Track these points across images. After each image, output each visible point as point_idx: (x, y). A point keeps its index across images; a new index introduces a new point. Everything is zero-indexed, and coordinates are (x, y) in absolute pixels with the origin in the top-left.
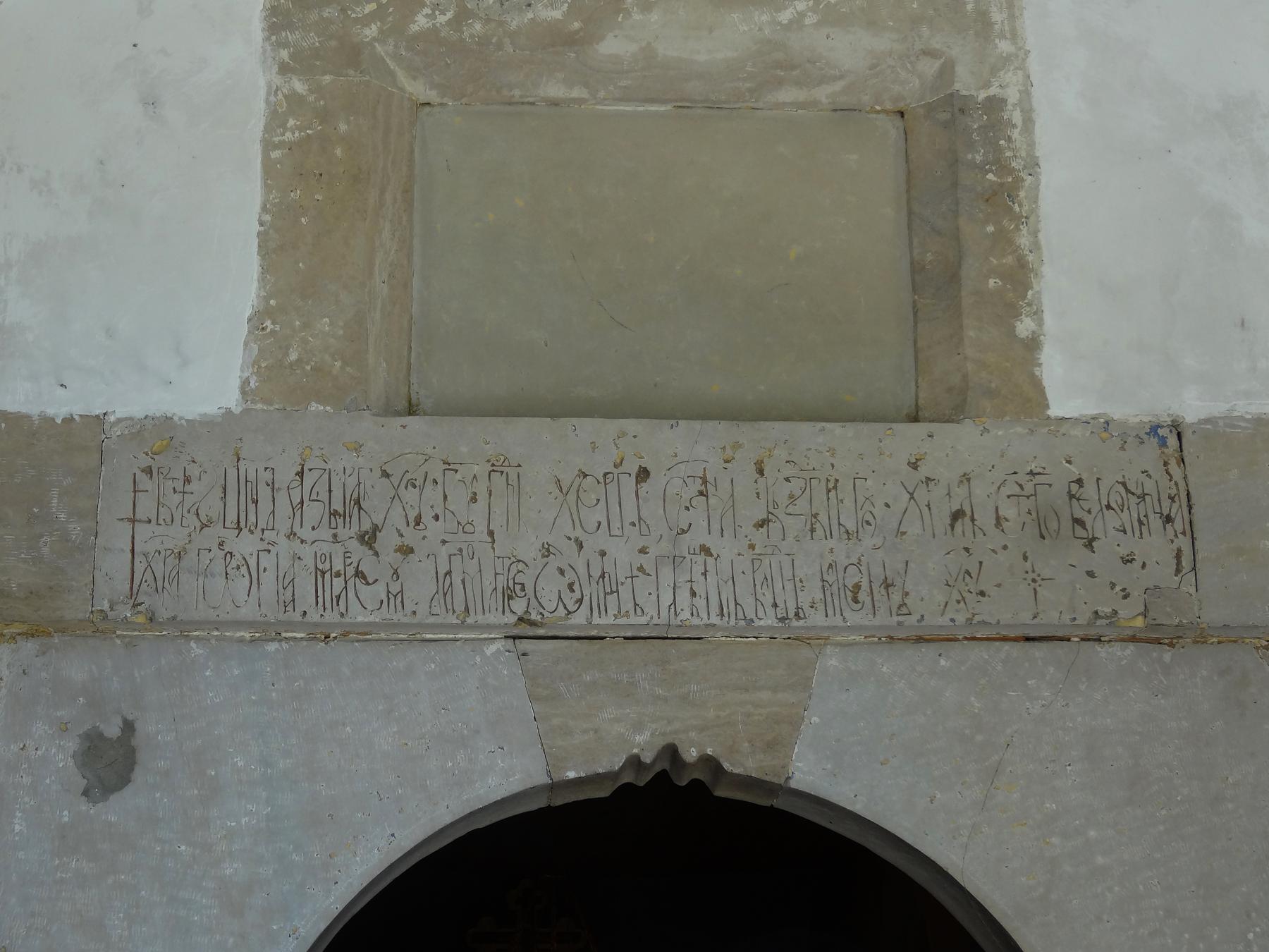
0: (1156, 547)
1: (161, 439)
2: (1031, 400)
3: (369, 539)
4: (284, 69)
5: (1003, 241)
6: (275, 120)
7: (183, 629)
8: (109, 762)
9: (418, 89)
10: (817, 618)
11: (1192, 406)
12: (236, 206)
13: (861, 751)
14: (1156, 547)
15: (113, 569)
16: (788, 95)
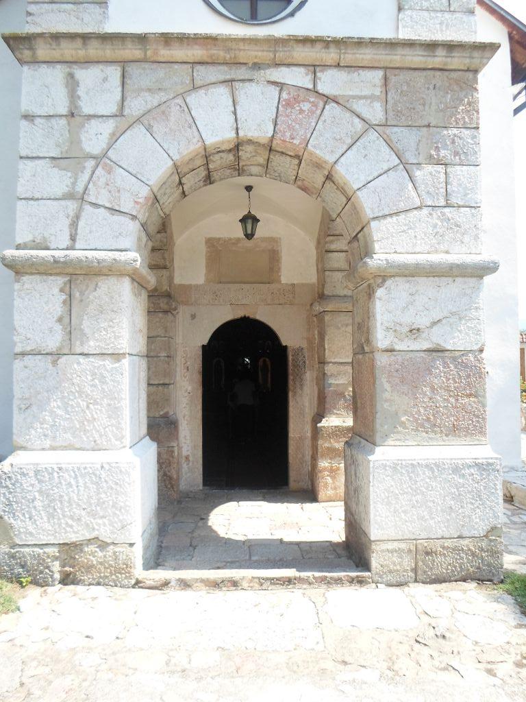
0: (291, 296)
1: (197, 286)
3: (217, 296)
4: (207, 248)
5: (278, 265)
6: (207, 253)
7: (199, 305)
8: (193, 317)
9: (220, 249)
10: (259, 303)
11: (295, 282)
12: (203, 262)
13: (263, 315)
14: (291, 296)
15: (193, 299)
16: (258, 249)
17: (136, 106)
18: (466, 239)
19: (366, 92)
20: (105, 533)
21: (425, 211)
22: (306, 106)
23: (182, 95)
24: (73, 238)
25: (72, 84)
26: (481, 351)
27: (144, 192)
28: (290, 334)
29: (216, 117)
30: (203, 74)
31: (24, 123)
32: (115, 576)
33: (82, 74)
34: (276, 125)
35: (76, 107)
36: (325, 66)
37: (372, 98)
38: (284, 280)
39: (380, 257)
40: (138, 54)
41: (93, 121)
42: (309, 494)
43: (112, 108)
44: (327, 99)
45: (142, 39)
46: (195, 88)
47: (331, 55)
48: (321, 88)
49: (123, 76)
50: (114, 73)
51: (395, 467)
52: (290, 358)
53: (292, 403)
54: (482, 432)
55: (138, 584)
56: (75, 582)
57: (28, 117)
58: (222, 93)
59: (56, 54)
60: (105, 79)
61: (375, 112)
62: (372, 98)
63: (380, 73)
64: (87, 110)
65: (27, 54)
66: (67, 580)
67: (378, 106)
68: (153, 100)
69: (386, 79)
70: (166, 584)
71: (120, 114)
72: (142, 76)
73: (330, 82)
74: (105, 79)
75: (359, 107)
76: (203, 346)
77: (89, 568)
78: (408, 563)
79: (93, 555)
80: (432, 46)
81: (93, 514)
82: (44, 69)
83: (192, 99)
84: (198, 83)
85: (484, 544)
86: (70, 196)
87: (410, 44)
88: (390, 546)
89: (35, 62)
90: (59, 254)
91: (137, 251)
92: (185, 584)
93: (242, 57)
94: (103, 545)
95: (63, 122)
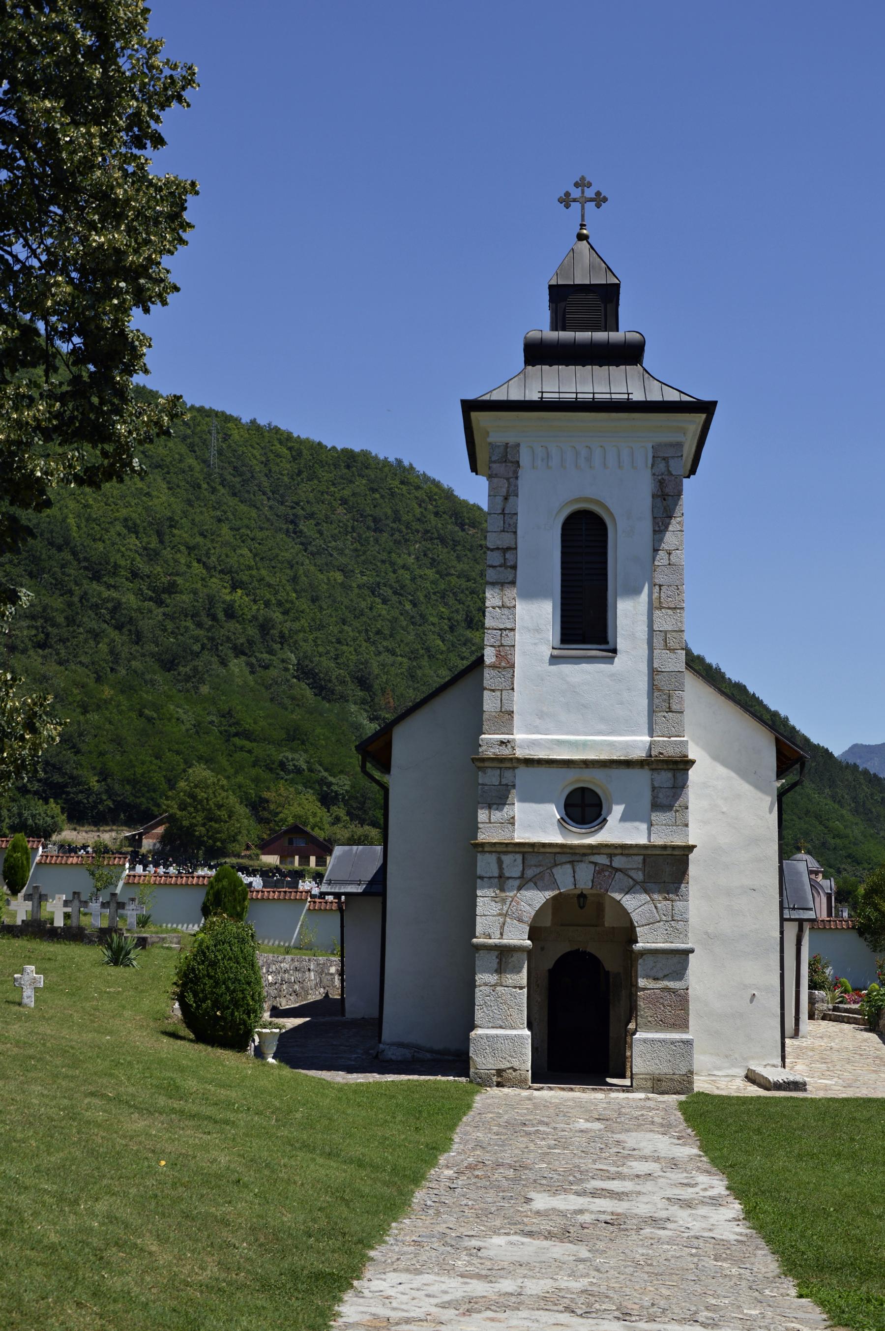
1: (546, 928)
2: (603, 925)
13: (592, 948)
17: (529, 873)
18: (681, 936)
19: (635, 867)
20: (516, 1064)
21: (662, 923)
22: (607, 874)
23: (551, 868)
24: (502, 934)
25: (500, 862)
26: (687, 989)
27: (533, 913)
28: (611, 963)
29: (566, 880)
30: (561, 859)
31: (479, 881)
32: (520, 1083)
33: (504, 857)
34: (593, 882)
35: (503, 873)
36: (615, 855)
37: (638, 869)
38: (607, 925)
39: (639, 946)
40: (531, 850)
41: (510, 880)
42: (623, 1076)
43: (518, 874)
44: (617, 870)
45: (533, 845)
46: (556, 865)
47: (619, 851)
48: (614, 865)
49: (523, 859)
50: (519, 857)
51: (645, 1041)
52: (611, 980)
53: (611, 1013)
54: (688, 1028)
55: (530, 1088)
56: (503, 1086)
57: (482, 878)
58: (568, 868)
59: (494, 850)
60: (515, 860)
61: (639, 876)
62: (638, 869)
63: (642, 857)
64: (507, 875)
65: (480, 849)
66: (499, 1085)
67: (640, 873)
68: (537, 870)
69: (644, 860)
70: (542, 1088)
71: (522, 877)
72: (532, 860)
73: (618, 862)
74: (515, 860)
75: (632, 873)
76: (549, 971)
77: (509, 1080)
78: (649, 1084)
79: (510, 1074)
80: (665, 847)
81: (510, 1056)
82: (487, 855)
83: (554, 871)
84: (557, 863)
85: (685, 1078)
86: (500, 915)
87: (655, 847)
88: (641, 1076)
89: (483, 852)
90: (497, 941)
91: (529, 939)
92: (551, 1089)
93: (577, 851)
94: (515, 1070)
95: (496, 880)
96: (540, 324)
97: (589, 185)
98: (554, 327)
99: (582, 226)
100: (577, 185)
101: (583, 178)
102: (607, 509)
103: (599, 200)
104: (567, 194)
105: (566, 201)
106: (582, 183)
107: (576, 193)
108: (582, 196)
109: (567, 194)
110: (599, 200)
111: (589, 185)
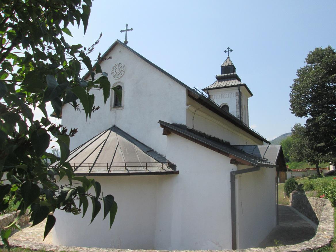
96: (219, 73)
97: (229, 48)
98: (222, 74)
99: (228, 55)
100: (227, 49)
101: (228, 47)
102: (223, 103)
103: (231, 51)
104: (226, 50)
105: (226, 52)
106: (228, 48)
107: (227, 50)
108: (229, 50)
109: (226, 50)
110: (231, 51)
111: (229, 48)
